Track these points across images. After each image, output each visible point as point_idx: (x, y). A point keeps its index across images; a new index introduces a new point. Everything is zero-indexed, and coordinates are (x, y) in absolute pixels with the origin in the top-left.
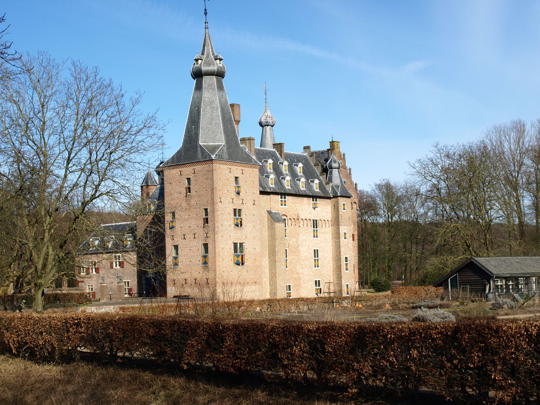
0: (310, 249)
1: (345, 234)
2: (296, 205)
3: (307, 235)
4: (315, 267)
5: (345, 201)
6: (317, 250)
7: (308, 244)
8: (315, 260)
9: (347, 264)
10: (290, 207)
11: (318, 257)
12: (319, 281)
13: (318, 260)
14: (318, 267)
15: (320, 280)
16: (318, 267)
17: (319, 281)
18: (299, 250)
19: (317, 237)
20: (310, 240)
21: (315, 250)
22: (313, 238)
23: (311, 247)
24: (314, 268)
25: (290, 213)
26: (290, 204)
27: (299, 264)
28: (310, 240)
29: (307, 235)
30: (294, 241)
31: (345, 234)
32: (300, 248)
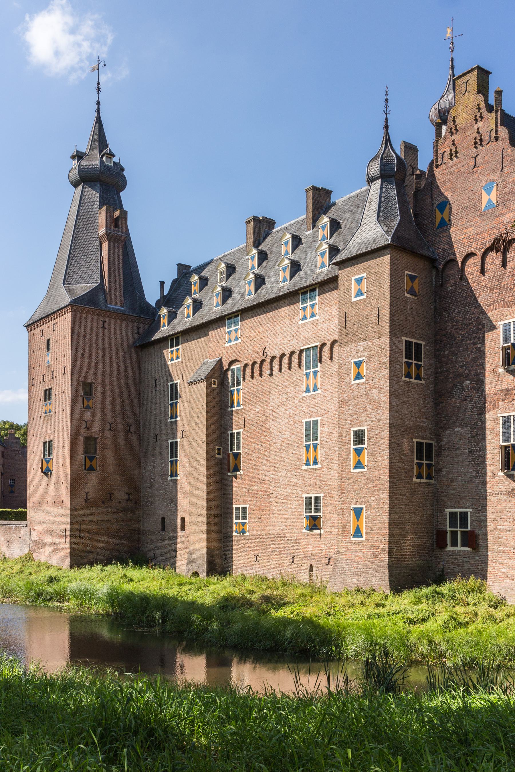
0: (295, 422)
1: (358, 364)
2: (261, 329)
3: (289, 391)
4: (308, 463)
5: (364, 270)
6: (315, 422)
7: (290, 411)
8: (308, 447)
9: (359, 452)
10: (246, 339)
11: (315, 439)
12: (317, 499)
13: (315, 446)
14: (315, 463)
15: (322, 495)
16: (315, 463)
17: (317, 499)
18: (268, 429)
19: (315, 389)
20: (296, 402)
21: (308, 424)
22: (304, 394)
23: (297, 418)
24: (304, 467)
25: (246, 352)
26: (247, 332)
27: (267, 461)
28: (296, 402)
29: (288, 390)
30: (257, 410)
31: (358, 364)
32: (271, 424)
